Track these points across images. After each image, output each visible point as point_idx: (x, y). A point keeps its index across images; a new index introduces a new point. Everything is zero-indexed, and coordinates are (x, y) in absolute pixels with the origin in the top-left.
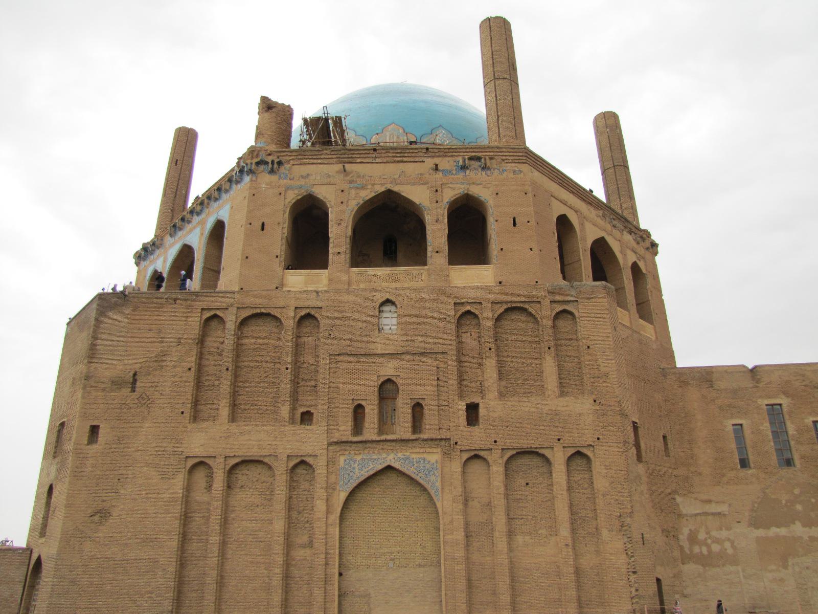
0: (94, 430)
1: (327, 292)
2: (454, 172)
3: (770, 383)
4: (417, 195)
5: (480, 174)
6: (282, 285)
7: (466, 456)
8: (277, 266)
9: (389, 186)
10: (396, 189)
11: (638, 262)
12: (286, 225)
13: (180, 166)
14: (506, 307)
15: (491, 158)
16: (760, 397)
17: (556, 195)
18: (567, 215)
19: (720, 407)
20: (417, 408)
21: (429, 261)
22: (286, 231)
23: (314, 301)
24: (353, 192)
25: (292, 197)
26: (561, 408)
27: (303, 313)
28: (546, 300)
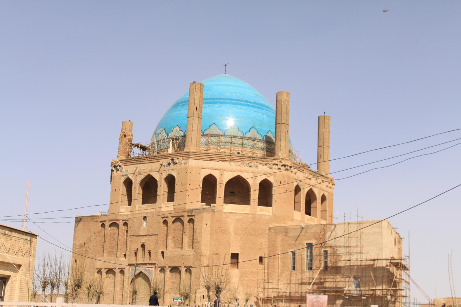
0: (76, 261)
3: (310, 233)
4: (156, 176)
7: (159, 269)
9: (148, 173)
10: (151, 174)
11: (268, 179)
15: (178, 159)
16: (305, 240)
17: (205, 167)
19: (288, 244)
20: (150, 253)
23: (126, 218)
25: (123, 179)
26: (185, 254)
27: (124, 222)
28: (186, 214)
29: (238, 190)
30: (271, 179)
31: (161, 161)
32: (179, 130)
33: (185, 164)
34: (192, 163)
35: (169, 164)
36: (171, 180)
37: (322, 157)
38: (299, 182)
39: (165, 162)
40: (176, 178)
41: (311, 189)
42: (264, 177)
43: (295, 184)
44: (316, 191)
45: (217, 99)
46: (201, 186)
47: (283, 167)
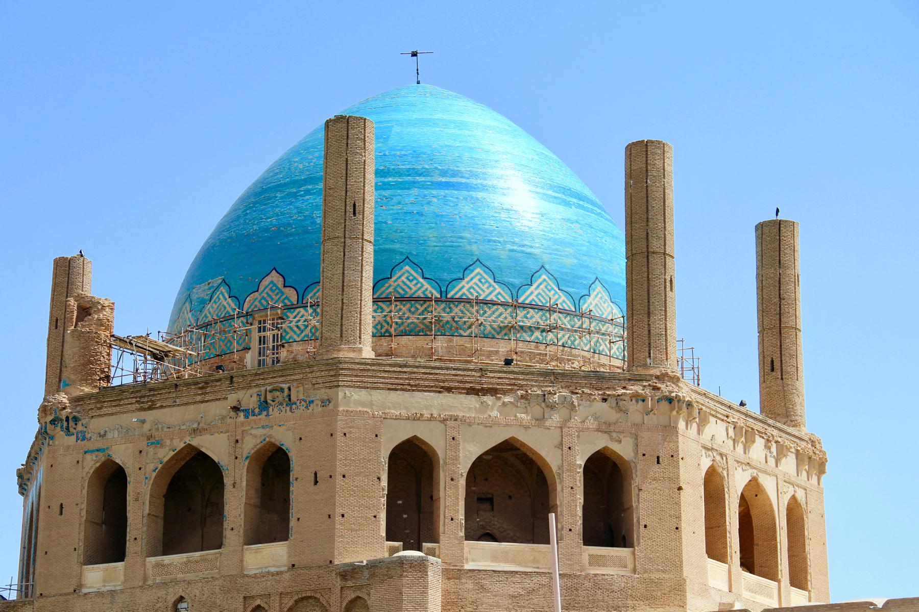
1: (122, 591)
2: (257, 410)
4: (216, 447)
5: (284, 410)
6: (81, 586)
8: (76, 557)
9: (188, 440)
10: (194, 443)
11: (615, 447)
12: (84, 506)
13: (62, 329)
14: (296, 598)
18: (418, 435)
21: (226, 541)
22: (84, 513)
24: (151, 450)
25: (91, 463)
29: (511, 493)
30: (623, 449)
31: (232, 399)
32: (280, 285)
33: (326, 402)
34: (353, 399)
35: (264, 405)
36: (273, 467)
37: (777, 364)
38: (718, 458)
39: (249, 398)
40: (293, 455)
41: (754, 481)
42: (600, 443)
43: (706, 463)
44: (768, 484)
45: (409, 172)
46: (384, 483)
47: (665, 405)
